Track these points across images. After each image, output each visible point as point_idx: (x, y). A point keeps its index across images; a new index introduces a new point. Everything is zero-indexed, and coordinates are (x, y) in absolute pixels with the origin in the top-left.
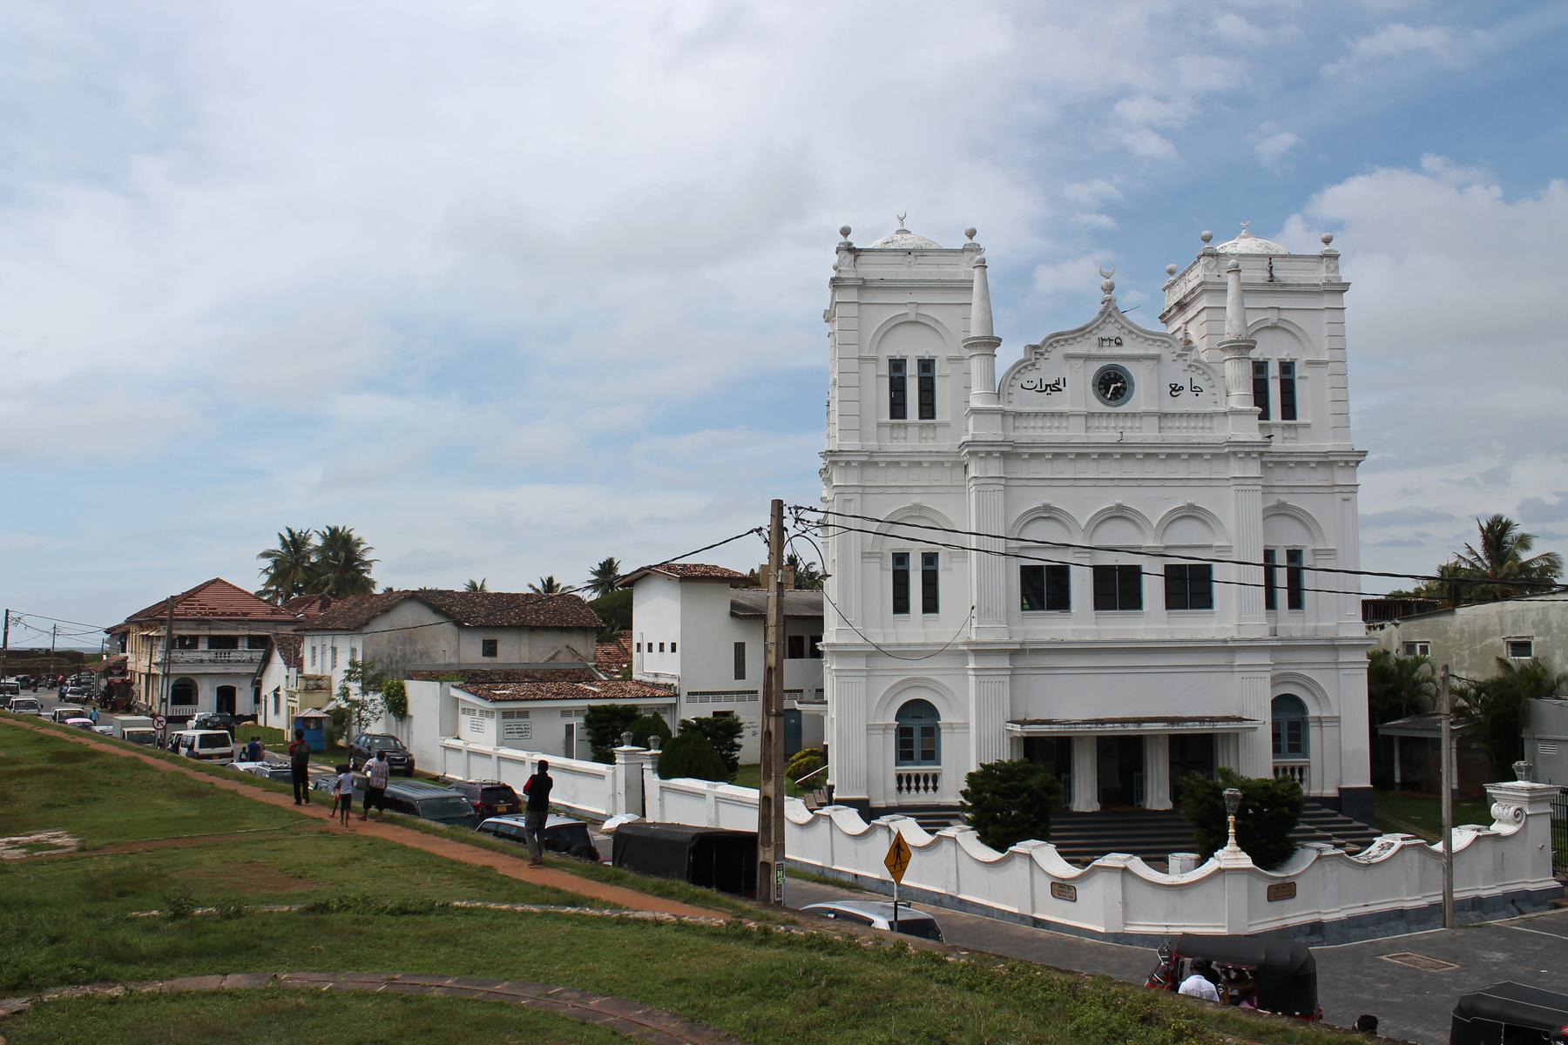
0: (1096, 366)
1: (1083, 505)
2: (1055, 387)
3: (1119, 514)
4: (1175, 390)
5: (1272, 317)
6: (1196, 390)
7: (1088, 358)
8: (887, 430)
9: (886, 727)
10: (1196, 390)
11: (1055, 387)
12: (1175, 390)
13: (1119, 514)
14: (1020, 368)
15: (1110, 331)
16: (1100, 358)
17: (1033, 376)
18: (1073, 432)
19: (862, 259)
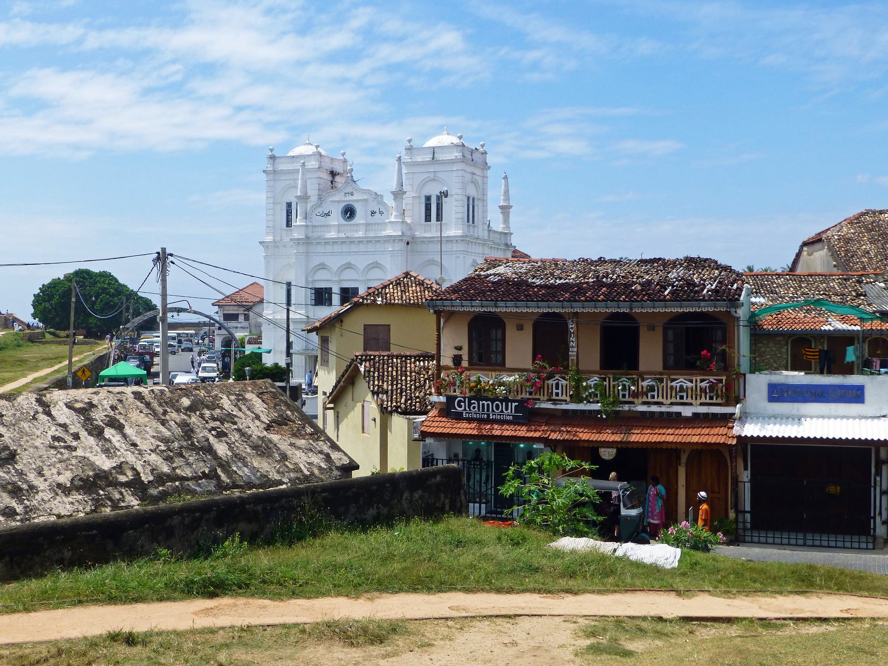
0: (342, 205)
1: (335, 263)
2: (328, 214)
3: (349, 266)
4: (373, 213)
5: (432, 175)
6: (381, 213)
7: (339, 202)
8: (285, 232)
9: (281, 352)
10: (381, 213)
11: (328, 214)
12: (373, 213)
13: (349, 266)
14: (315, 207)
15: (349, 190)
16: (344, 201)
17: (320, 210)
18: (333, 234)
19: (277, 161)
